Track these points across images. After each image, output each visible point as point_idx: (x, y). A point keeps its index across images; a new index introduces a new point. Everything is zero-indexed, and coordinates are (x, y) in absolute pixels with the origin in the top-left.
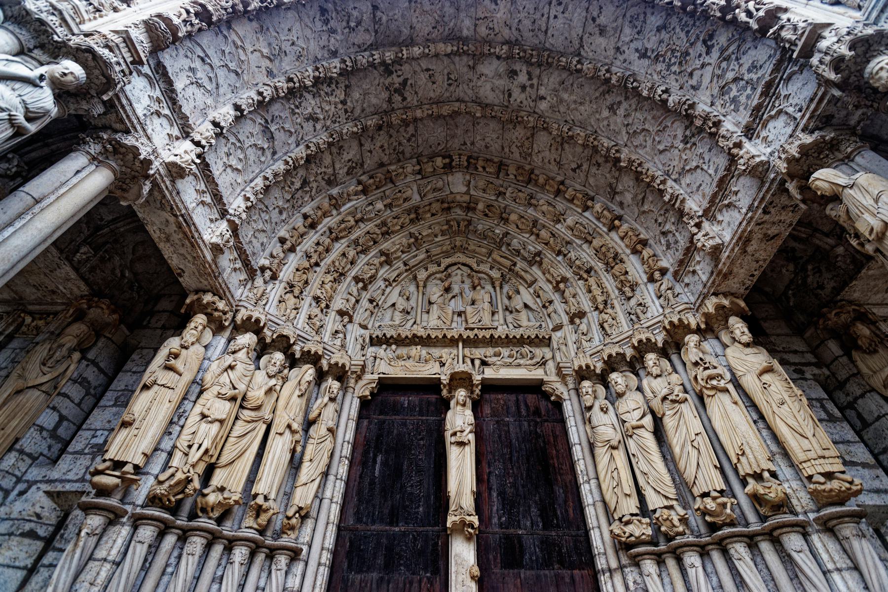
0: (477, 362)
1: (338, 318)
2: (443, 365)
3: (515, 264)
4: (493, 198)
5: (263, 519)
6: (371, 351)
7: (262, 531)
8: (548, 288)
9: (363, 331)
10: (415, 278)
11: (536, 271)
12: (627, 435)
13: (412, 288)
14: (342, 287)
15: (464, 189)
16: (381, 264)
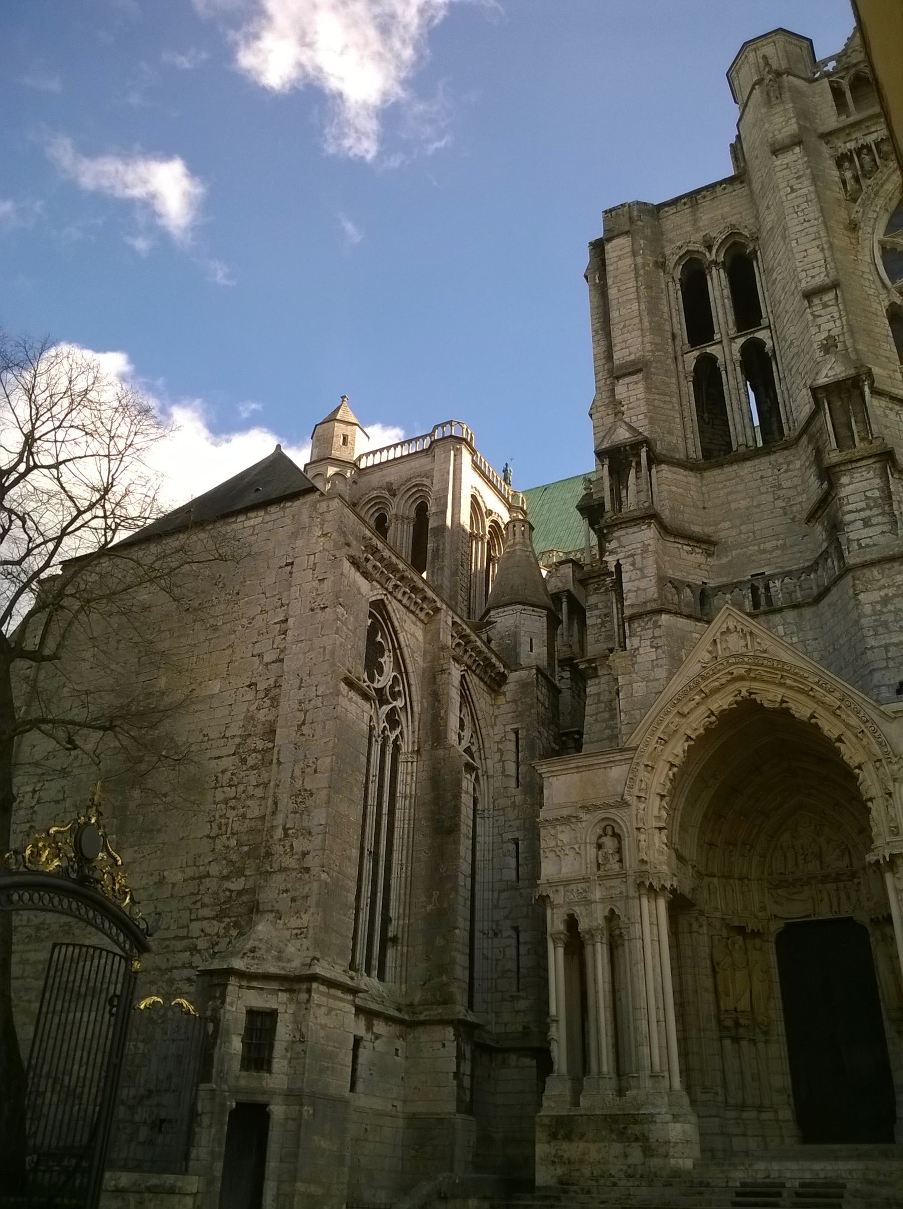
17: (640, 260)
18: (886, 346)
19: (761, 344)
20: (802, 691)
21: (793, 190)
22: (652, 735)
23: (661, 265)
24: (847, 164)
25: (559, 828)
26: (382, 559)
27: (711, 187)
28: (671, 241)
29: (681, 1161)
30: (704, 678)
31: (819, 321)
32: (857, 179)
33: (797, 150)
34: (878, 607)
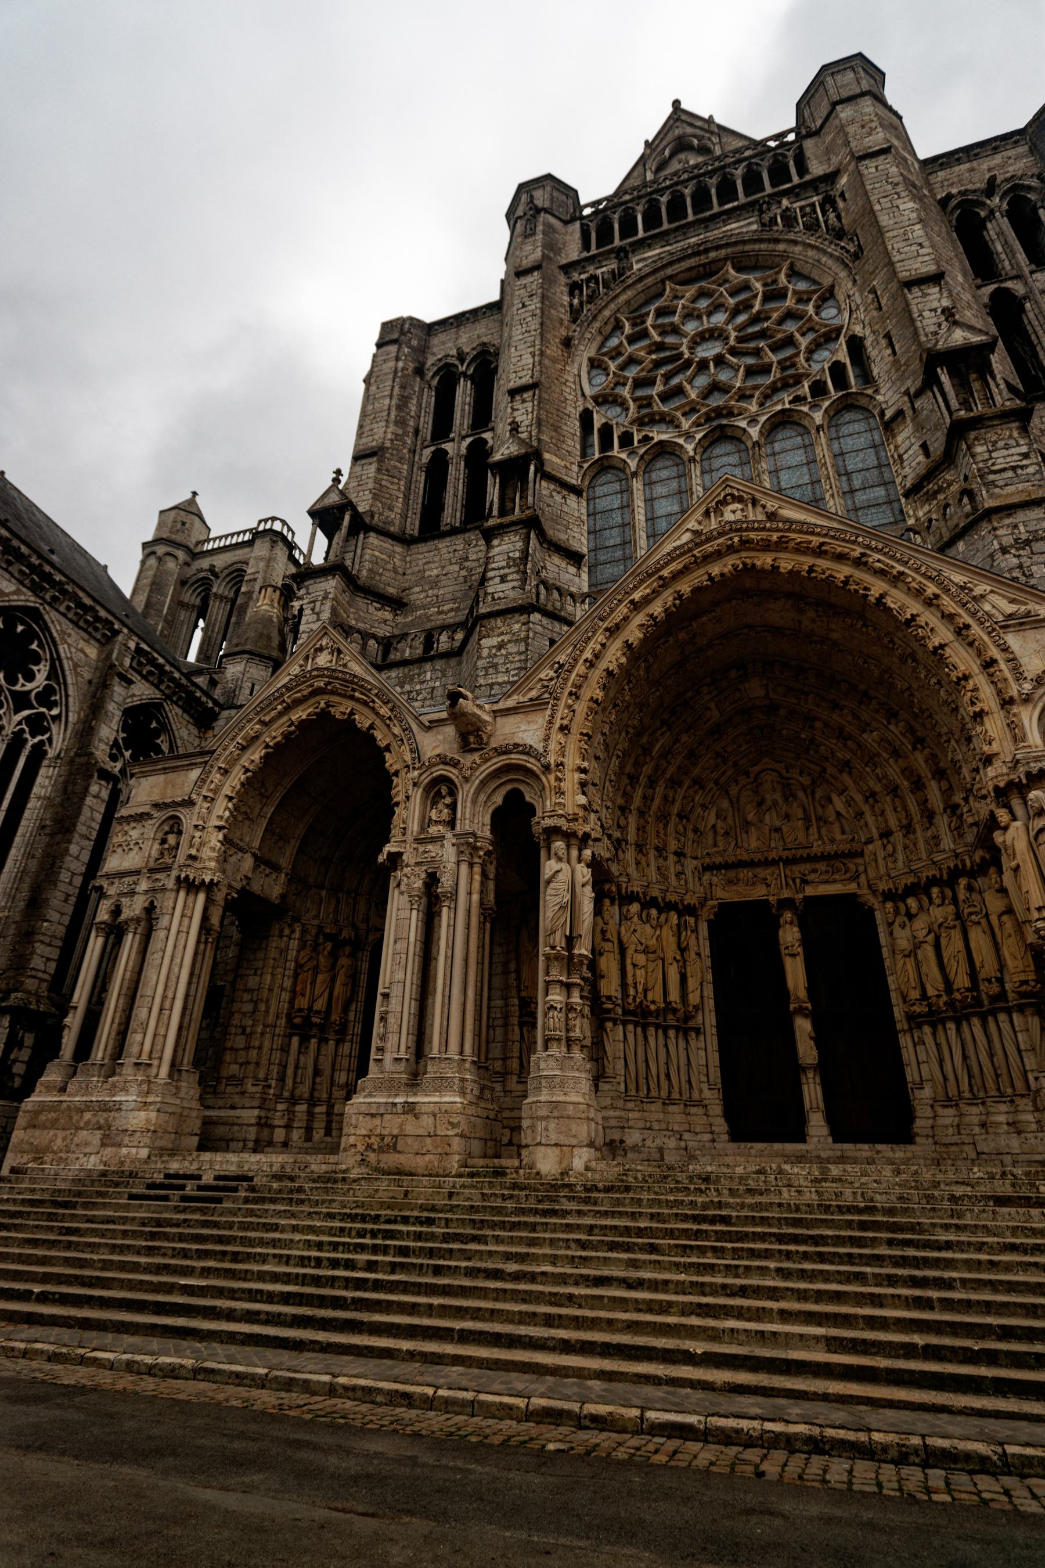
0: (798, 881)
1: (676, 858)
2: (768, 886)
3: (824, 770)
4: (794, 701)
5: (678, 1015)
6: (706, 877)
7: (678, 1020)
8: (859, 798)
9: (695, 862)
10: (727, 792)
11: (845, 777)
12: (917, 945)
13: (726, 804)
14: (671, 828)
15: (761, 693)
16: (696, 792)
17: (401, 364)
18: (570, 442)
19: (485, 442)
20: (365, 703)
21: (524, 306)
22: (232, 740)
23: (419, 371)
24: (577, 292)
25: (133, 825)
26: (30, 566)
27: (474, 312)
28: (434, 354)
29: (134, 1150)
30: (289, 690)
31: (516, 413)
32: (581, 304)
33: (536, 273)
34: (494, 651)
